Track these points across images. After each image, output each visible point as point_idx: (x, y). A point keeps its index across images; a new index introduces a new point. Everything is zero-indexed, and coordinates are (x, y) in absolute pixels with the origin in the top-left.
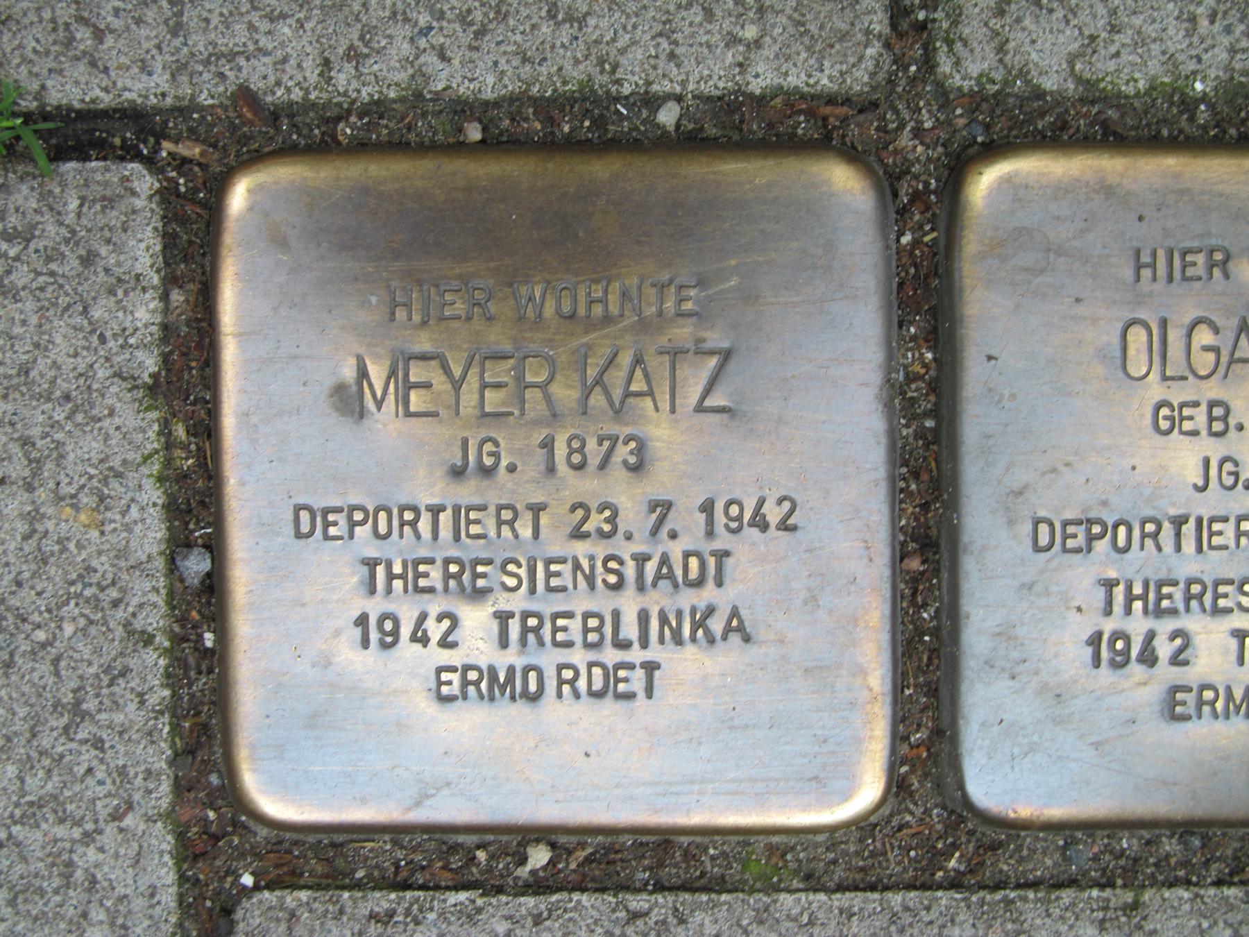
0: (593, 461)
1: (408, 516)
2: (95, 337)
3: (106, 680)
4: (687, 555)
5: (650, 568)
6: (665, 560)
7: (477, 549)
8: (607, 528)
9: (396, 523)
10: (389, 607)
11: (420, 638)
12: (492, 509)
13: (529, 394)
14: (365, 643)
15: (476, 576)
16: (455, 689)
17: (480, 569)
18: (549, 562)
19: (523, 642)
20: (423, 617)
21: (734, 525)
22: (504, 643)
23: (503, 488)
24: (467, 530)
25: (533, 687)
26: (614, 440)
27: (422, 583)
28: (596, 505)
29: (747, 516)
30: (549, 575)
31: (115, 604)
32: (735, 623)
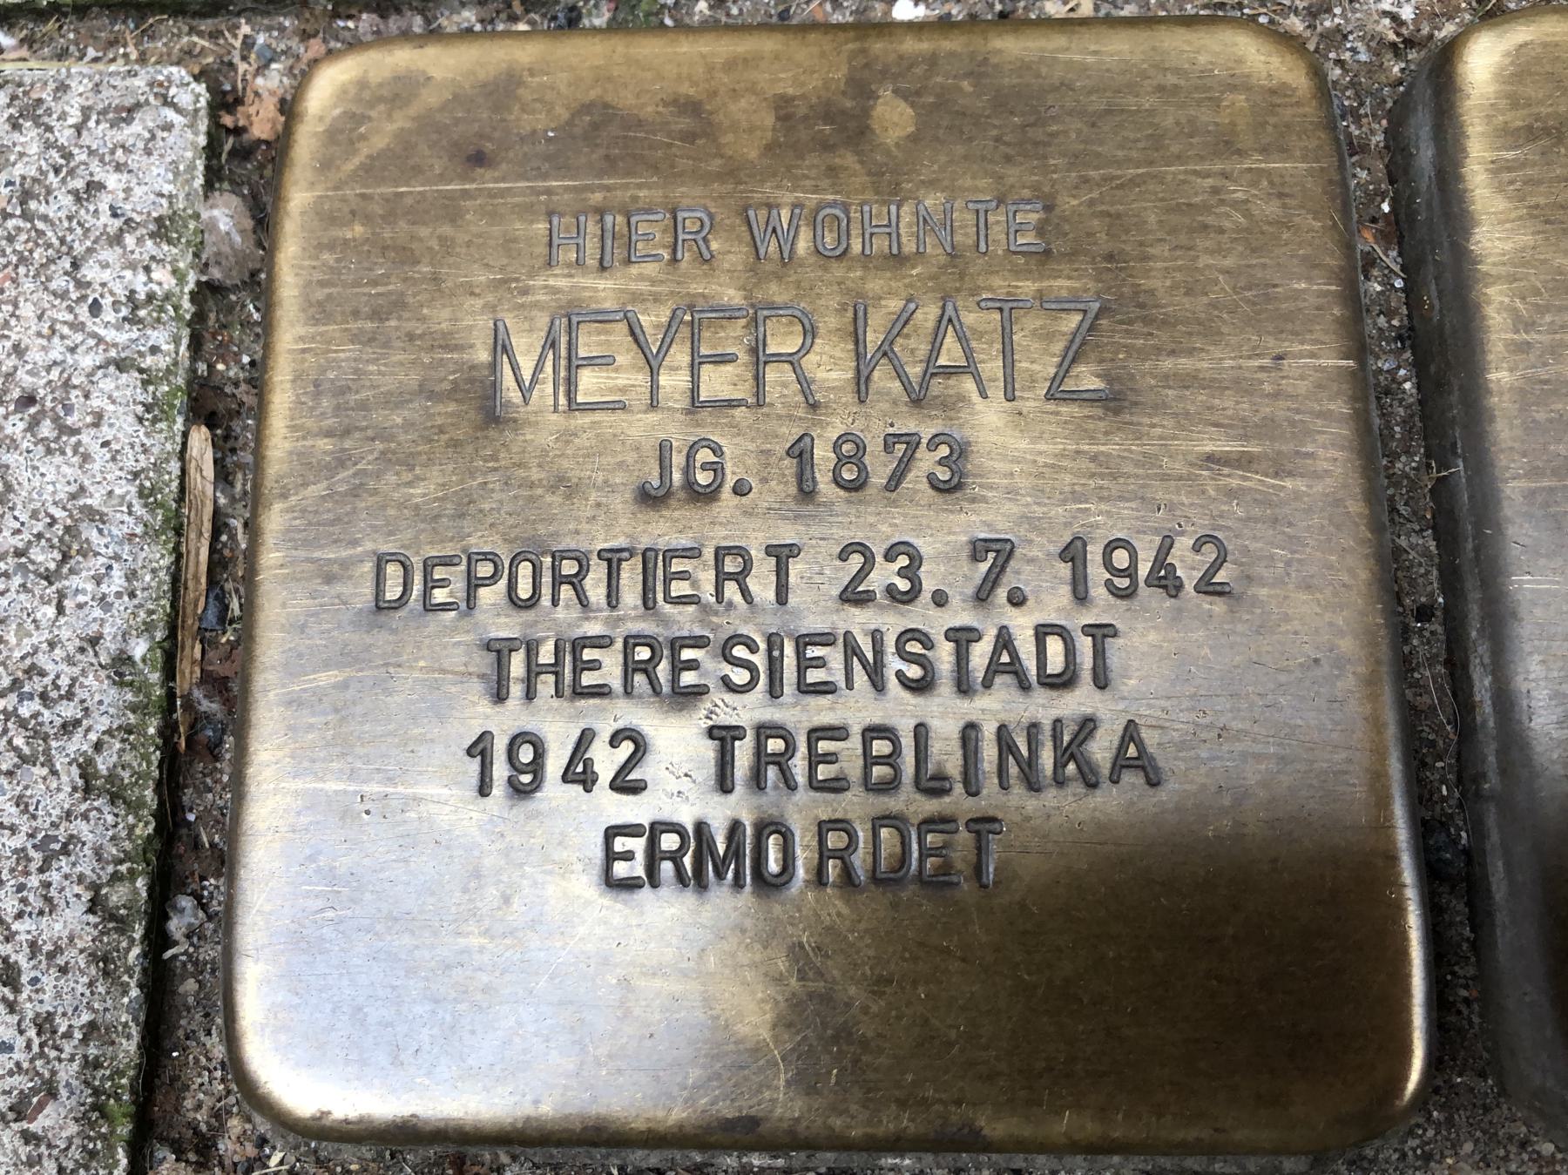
0: (879, 479)
1: (569, 568)
2: (86, 308)
3: (37, 856)
4: (1042, 632)
5: (980, 653)
6: (1004, 641)
7: (685, 620)
8: (903, 585)
9: (547, 579)
10: (529, 723)
11: (580, 774)
12: (708, 553)
13: (772, 374)
14: (484, 789)
15: (678, 667)
16: (638, 868)
17: (687, 654)
18: (803, 642)
19: (757, 780)
20: (585, 739)
21: (1123, 583)
22: (724, 783)
23: (724, 523)
24: (666, 591)
25: (773, 866)
26: (912, 442)
27: (588, 679)
28: (882, 551)
29: (1144, 570)
30: (803, 665)
31: (68, 727)
32: (1132, 751)
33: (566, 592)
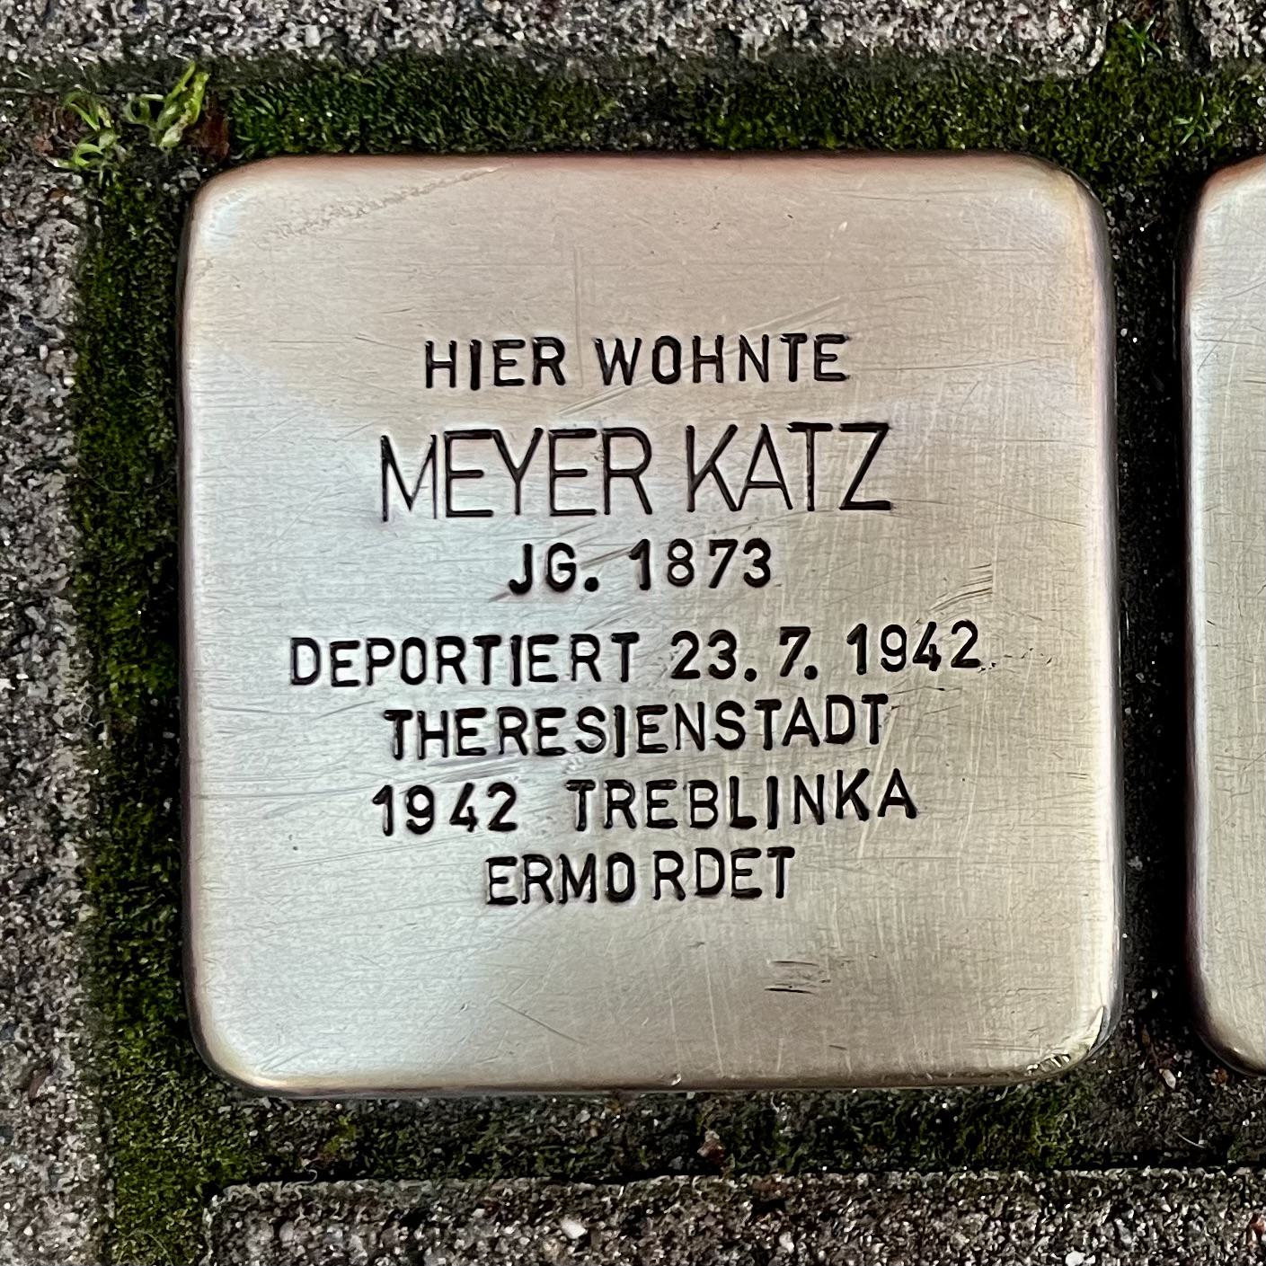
1: (450, 651)
5: (780, 720)
8: (723, 666)
33: (448, 670)
